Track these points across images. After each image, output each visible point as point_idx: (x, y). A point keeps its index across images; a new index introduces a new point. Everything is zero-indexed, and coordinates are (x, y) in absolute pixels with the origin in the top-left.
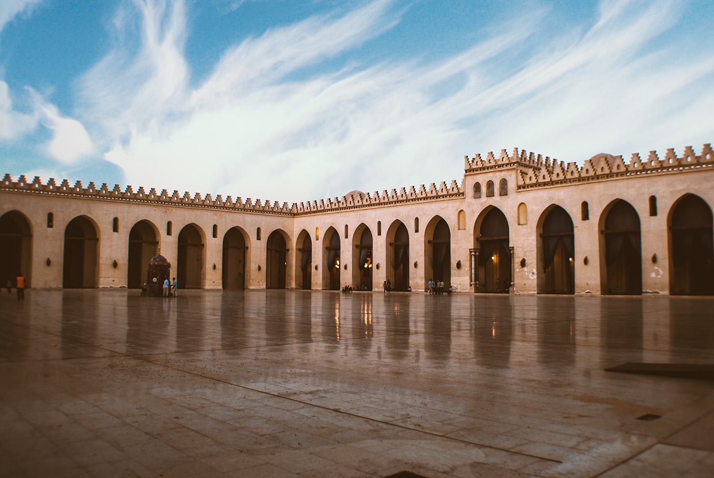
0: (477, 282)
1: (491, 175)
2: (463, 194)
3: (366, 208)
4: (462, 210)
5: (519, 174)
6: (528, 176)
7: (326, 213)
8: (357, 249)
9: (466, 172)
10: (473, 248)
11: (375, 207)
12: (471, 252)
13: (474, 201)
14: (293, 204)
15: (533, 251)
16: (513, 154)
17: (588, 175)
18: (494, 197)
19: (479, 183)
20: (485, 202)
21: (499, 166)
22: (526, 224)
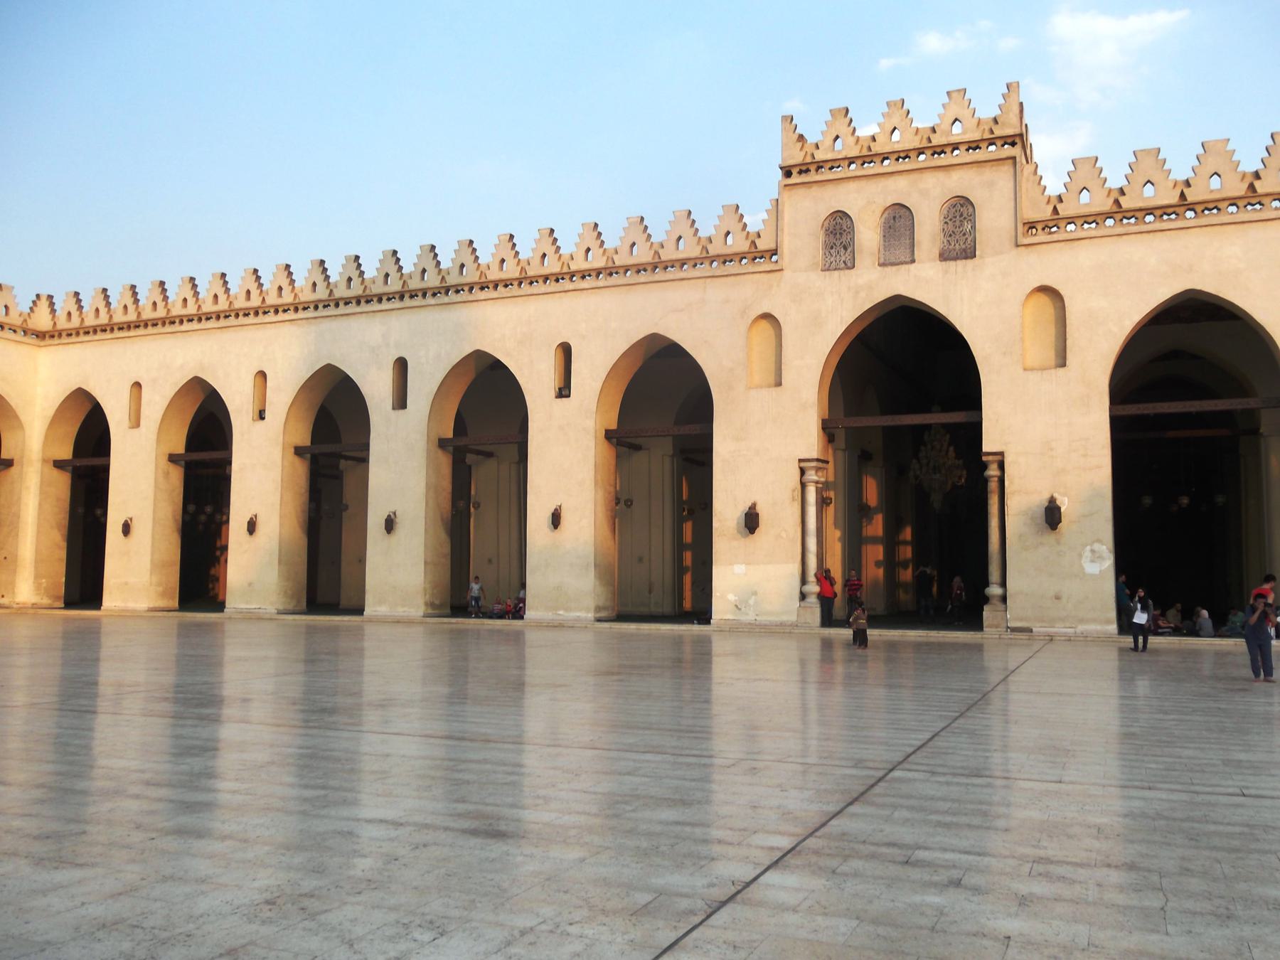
1: (901, 183)
2: (774, 252)
3: (342, 309)
4: (767, 316)
7: (177, 327)
8: (297, 460)
9: (788, 174)
10: (815, 455)
11: (385, 305)
12: (803, 472)
13: (821, 281)
14: (38, 296)
15: (1099, 467)
18: (913, 265)
19: (844, 215)
21: (939, 151)
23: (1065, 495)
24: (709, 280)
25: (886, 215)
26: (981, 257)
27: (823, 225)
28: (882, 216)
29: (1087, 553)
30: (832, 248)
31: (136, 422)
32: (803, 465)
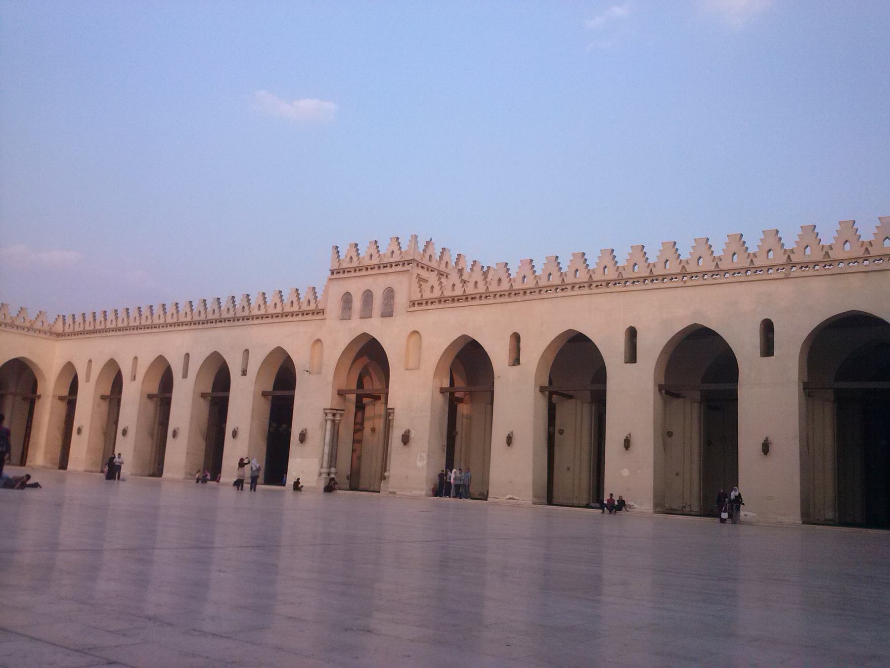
0: (333, 470)
2: (322, 312)
3: (169, 329)
4: (319, 340)
5: (415, 281)
6: (429, 285)
9: (333, 273)
10: (330, 408)
11: (185, 327)
12: (326, 414)
14: (58, 316)
16: (408, 246)
17: (525, 286)
20: (357, 327)
22: (418, 368)
23: (413, 429)
24: (300, 322)
25: (364, 295)
26: (395, 316)
27: (342, 298)
28: (363, 295)
29: (419, 457)
30: (345, 309)
31: (88, 380)
32: (326, 411)
